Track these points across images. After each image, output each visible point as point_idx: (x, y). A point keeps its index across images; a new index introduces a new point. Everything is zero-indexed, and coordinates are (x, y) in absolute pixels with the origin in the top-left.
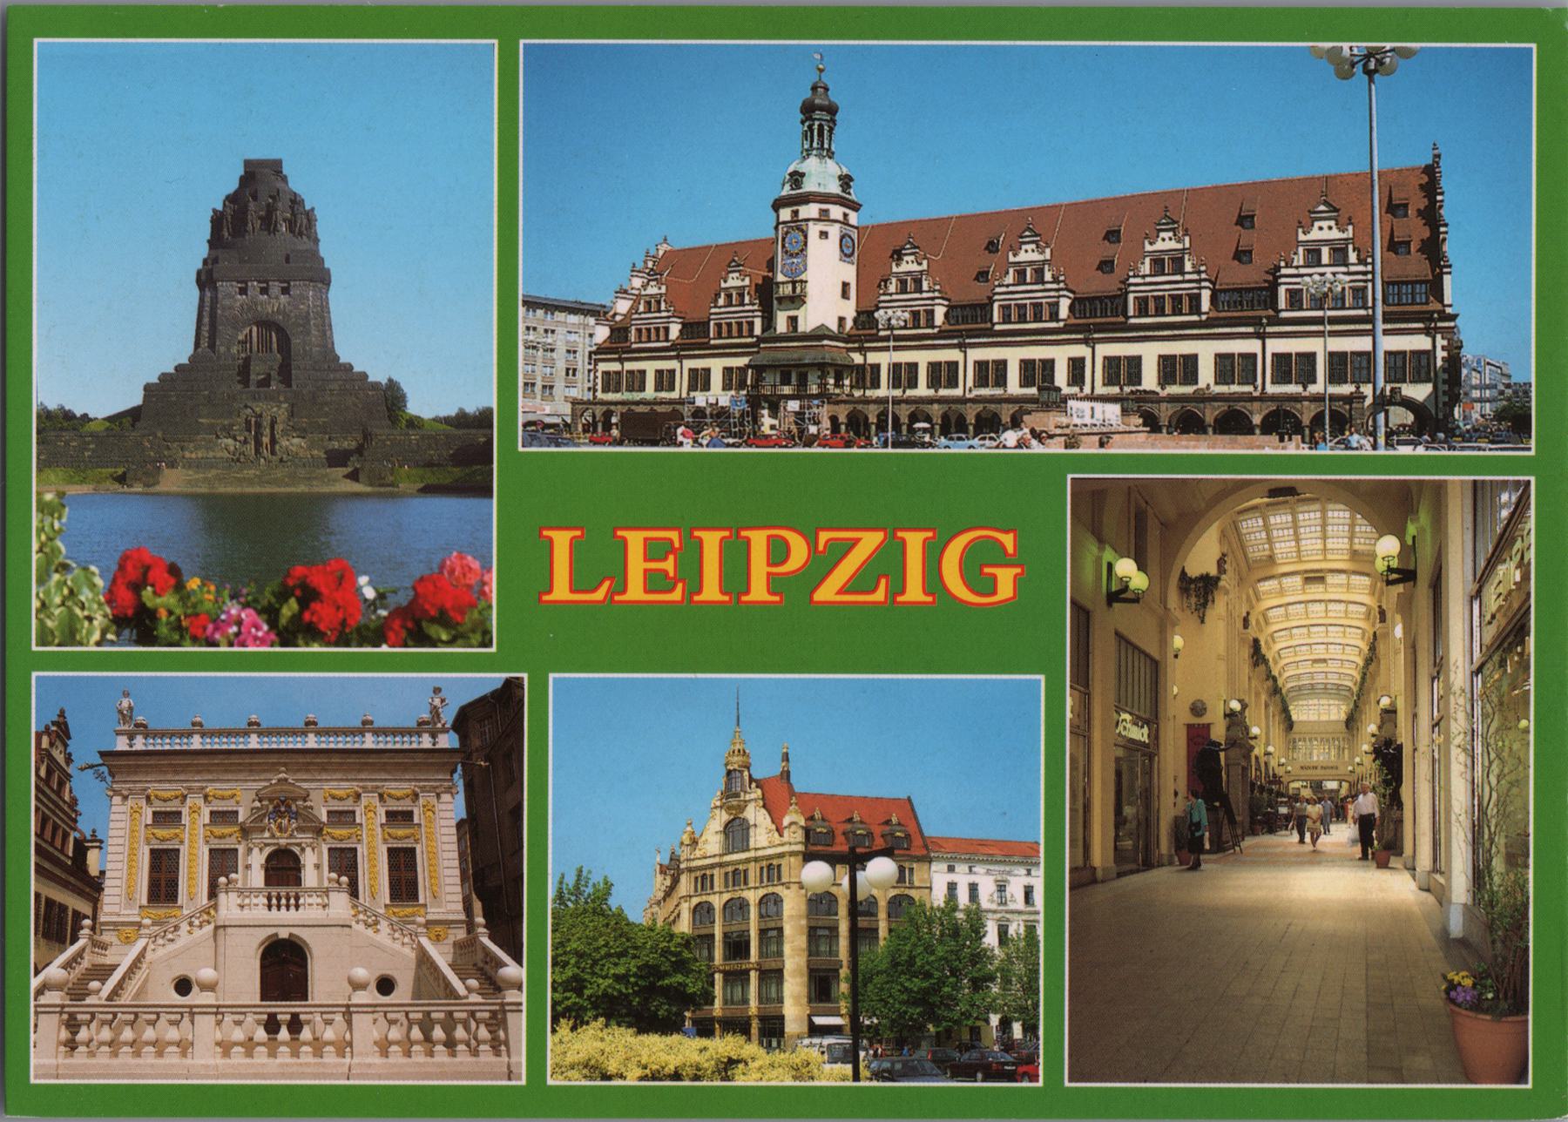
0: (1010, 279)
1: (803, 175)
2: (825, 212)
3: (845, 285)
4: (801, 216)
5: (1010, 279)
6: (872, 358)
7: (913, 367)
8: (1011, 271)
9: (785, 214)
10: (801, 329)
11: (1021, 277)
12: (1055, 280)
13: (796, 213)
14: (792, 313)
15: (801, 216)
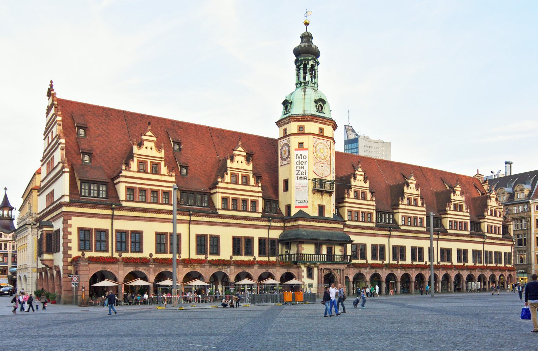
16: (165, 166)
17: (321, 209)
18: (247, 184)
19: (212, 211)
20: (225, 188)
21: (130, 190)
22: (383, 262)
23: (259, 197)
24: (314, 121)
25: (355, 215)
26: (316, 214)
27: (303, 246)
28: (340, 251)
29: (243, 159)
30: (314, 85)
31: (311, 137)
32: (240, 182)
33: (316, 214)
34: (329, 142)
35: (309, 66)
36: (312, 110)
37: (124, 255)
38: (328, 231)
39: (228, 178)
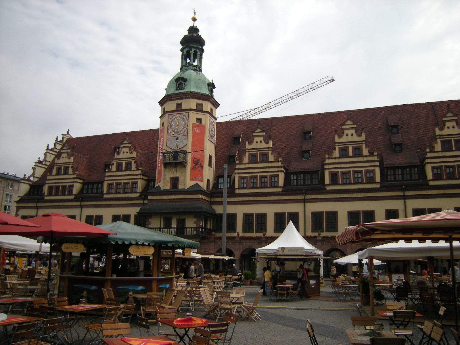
0: (336, 153)
1: (185, 80)
2: (200, 106)
3: (210, 157)
4: (184, 107)
5: (336, 153)
6: (231, 209)
7: (262, 217)
8: (337, 148)
9: (171, 106)
10: (180, 187)
11: (344, 152)
12: (371, 154)
13: (179, 105)
14: (174, 175)
15: (184, 107)
16: (72, 167)
17: (175, 181)
18: (131, 170)
19: (100, 197)
20: (113, 176)
21: (50, 188)
22: (264, 235)
23: (138, 179)
24: (170, 100)
25: (253, 182)
26: (168, 187)
27: (150, 220)
28: (195, 223)
29: (127, 149)
30: (188, 67)
31: (167, 115)
32: (124, 169)
33: (168, 187)
34: (186, 115)
35: (185, 53)
36: (173, 91)
37: (324, 234)
38: (178, 203)
39: (114, 168)
